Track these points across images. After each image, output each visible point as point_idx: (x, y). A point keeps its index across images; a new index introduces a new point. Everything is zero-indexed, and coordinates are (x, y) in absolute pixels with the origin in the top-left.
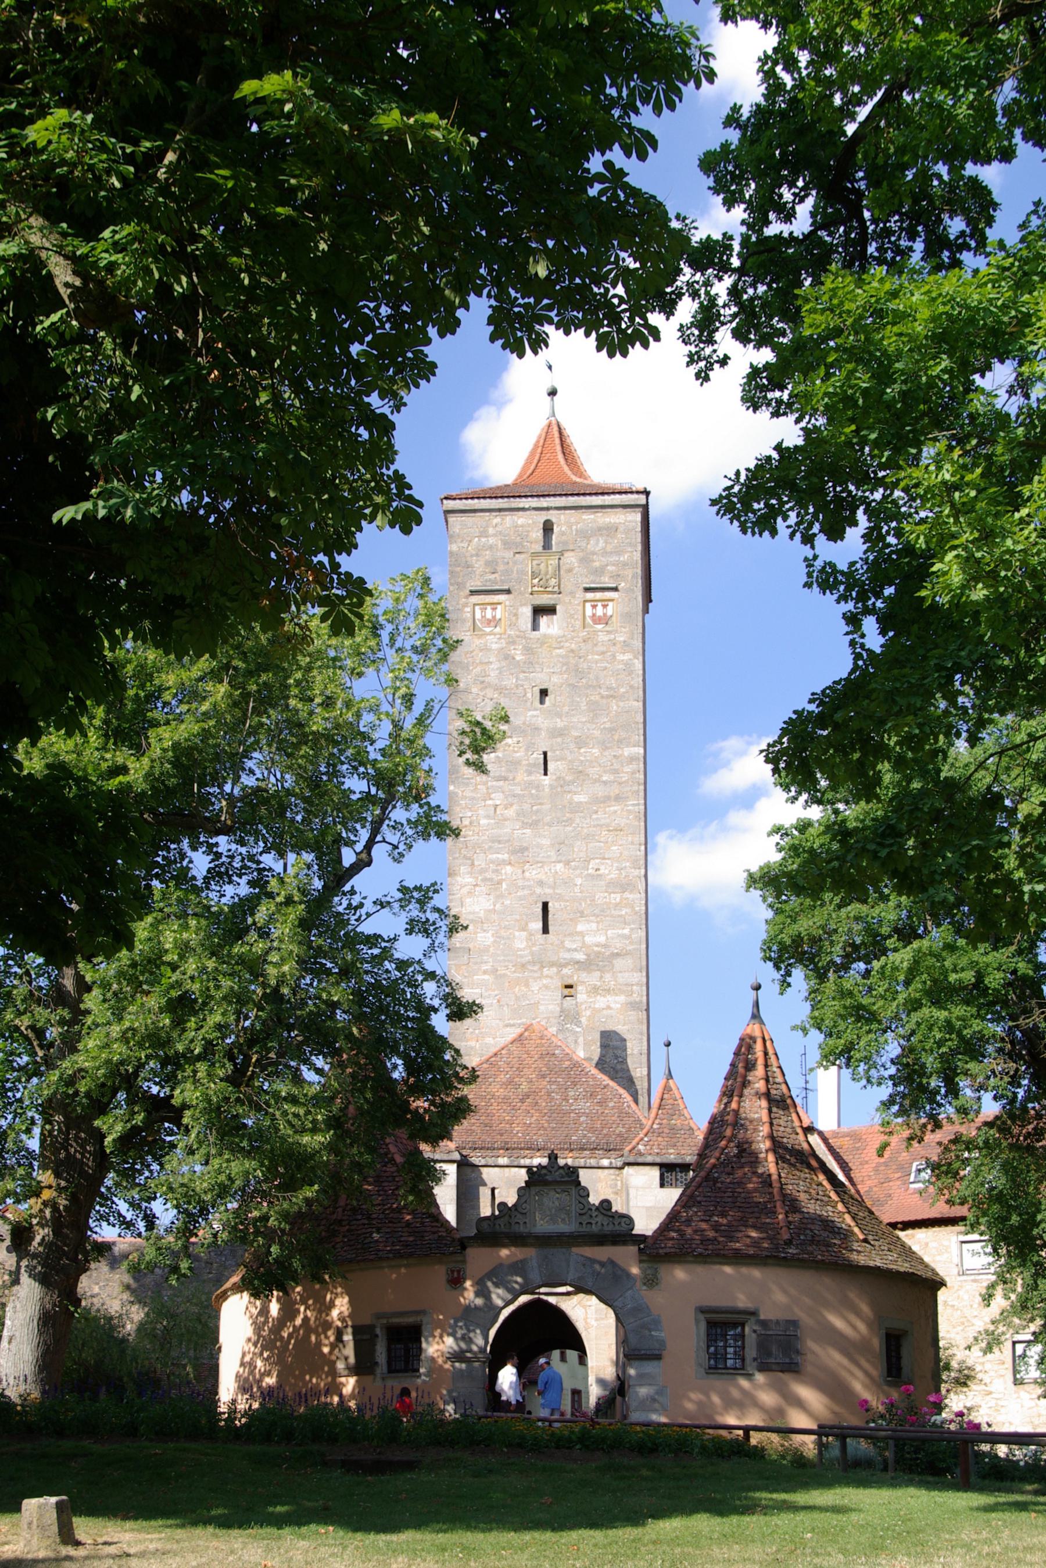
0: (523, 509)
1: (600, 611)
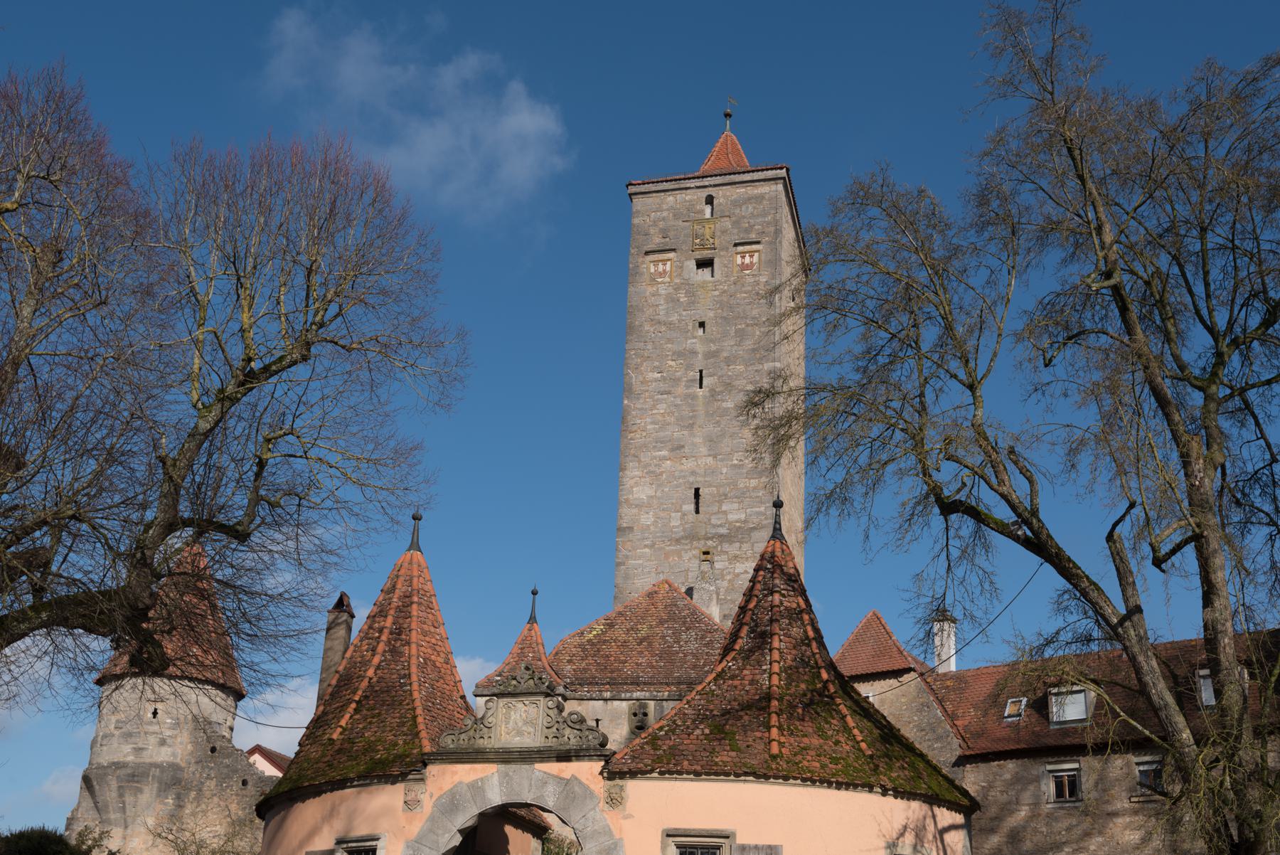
1: (747, 260)
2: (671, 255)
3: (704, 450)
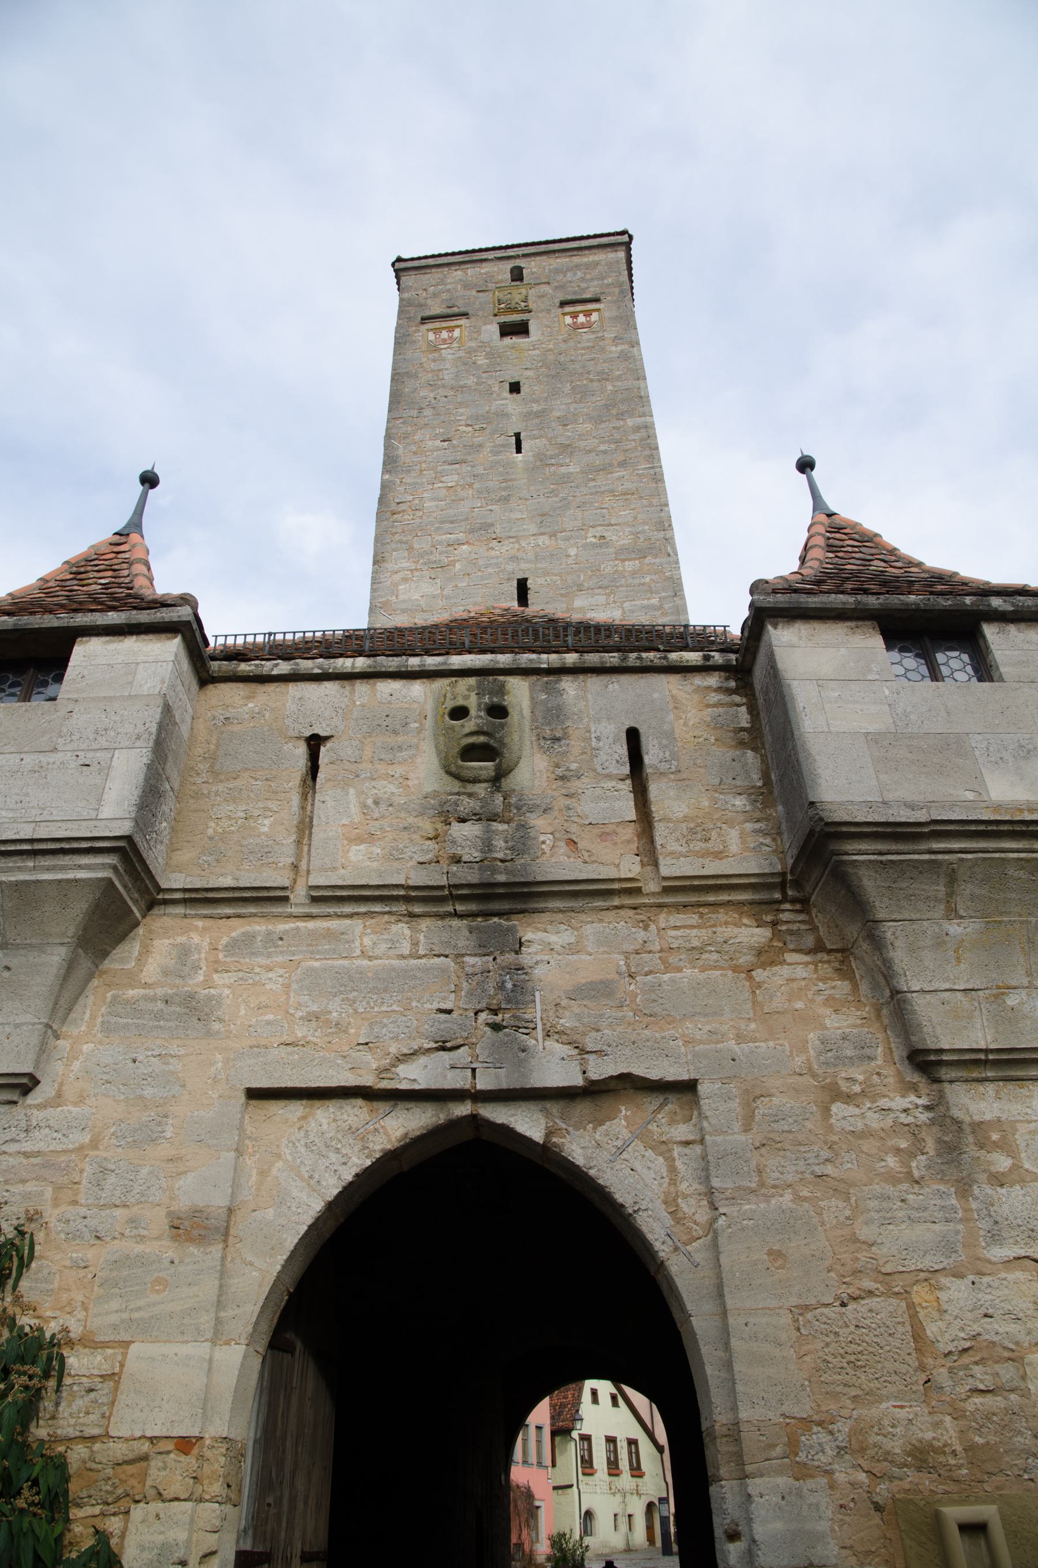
0: (486, 260)
2: (462, 322)
3: (533, 528)
